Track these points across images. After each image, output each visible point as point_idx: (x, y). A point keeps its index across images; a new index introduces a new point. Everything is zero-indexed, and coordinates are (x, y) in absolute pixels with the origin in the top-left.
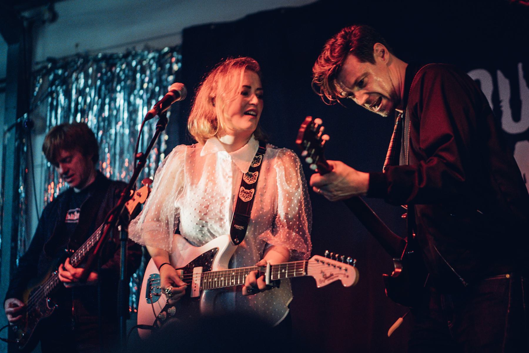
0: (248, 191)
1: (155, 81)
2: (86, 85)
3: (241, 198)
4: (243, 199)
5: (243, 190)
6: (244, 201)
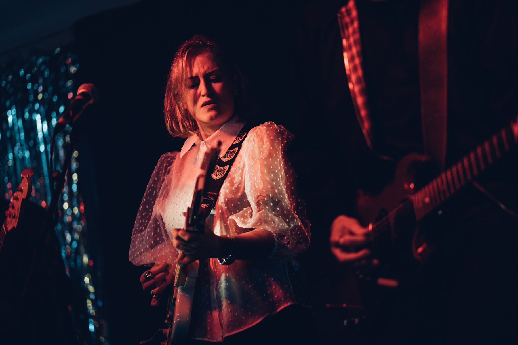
0: (222, 168)
1: (50, 89)
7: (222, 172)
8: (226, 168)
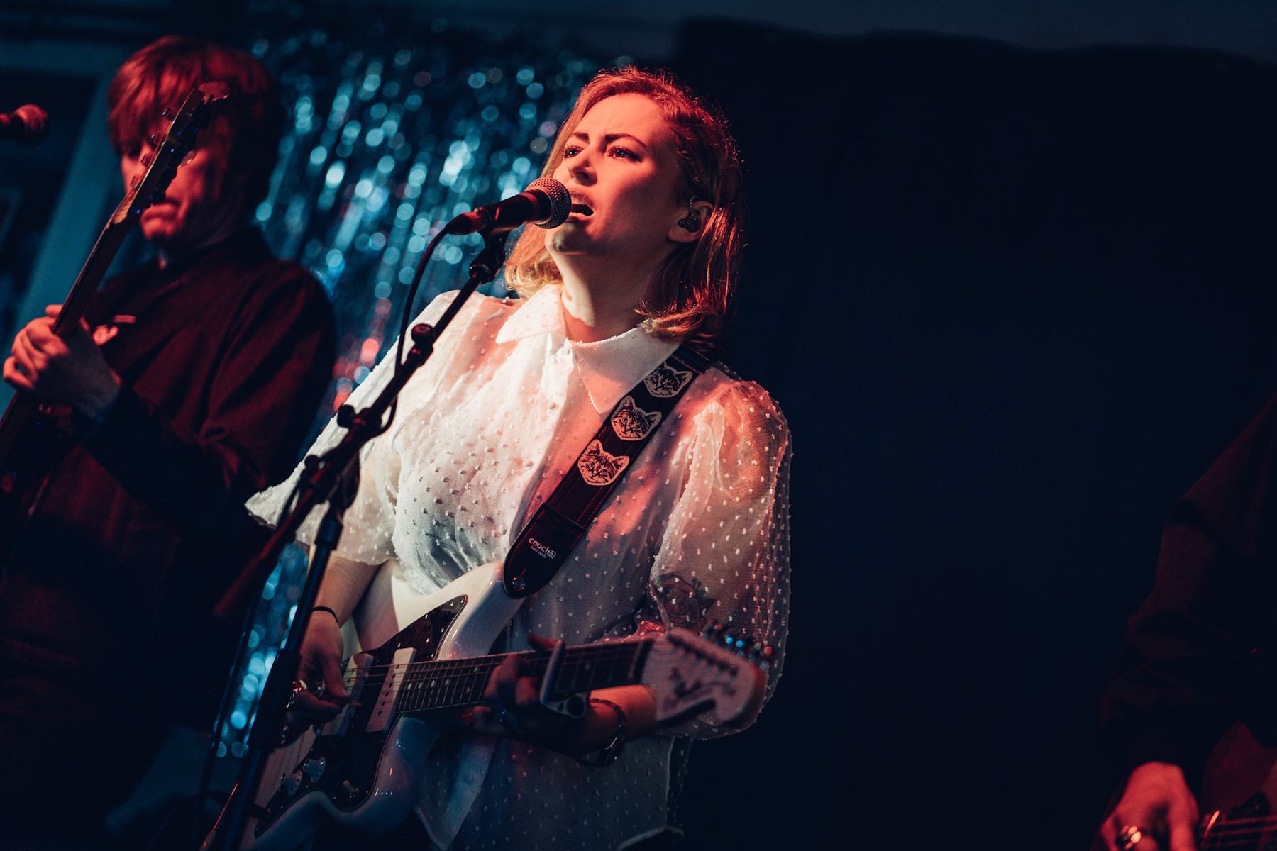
0: (611, 458)
2: (379, 97)
3: (581, 470)
4: (586, 474)
5: (598, 451)
6: (586, 480)
7: (609, 470)
8: (620, 463)
